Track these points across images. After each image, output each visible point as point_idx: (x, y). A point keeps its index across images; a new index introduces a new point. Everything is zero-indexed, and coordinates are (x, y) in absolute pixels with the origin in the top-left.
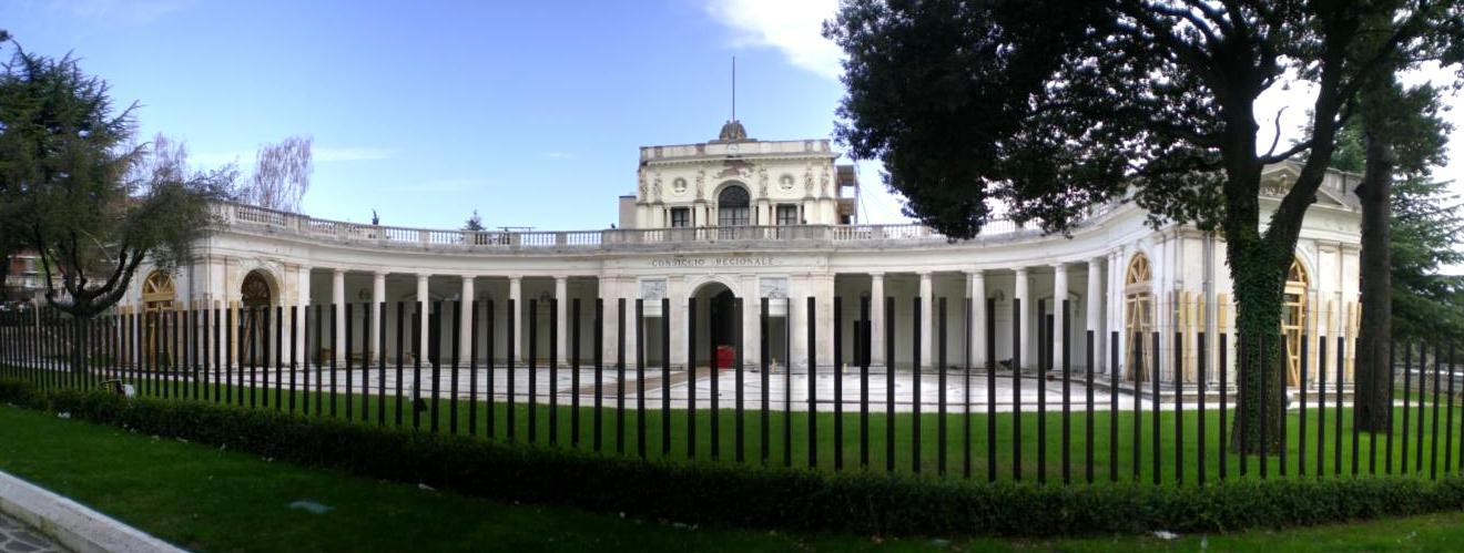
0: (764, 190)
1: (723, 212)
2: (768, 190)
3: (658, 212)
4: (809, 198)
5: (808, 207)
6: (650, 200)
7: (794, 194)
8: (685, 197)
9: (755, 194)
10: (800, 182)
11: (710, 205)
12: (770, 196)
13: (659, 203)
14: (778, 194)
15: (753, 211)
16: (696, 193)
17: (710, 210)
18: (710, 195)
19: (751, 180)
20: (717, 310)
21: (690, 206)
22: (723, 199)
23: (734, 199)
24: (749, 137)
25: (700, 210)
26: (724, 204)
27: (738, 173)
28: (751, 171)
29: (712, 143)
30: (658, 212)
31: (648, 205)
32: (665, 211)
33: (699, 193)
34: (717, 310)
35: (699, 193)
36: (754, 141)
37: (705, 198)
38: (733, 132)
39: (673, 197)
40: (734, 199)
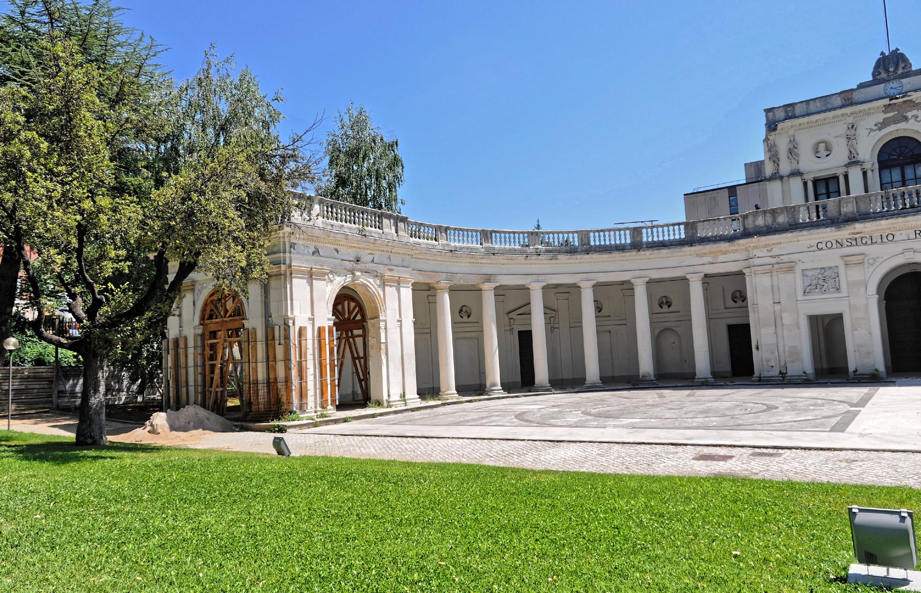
1: (886, 173)
3: (796, 183)
8: (833, 164)
11: (867, 166)
13: (796, 173)
16: (847, 153)
17: (869, 174)
21: (840, 172)
22: (886, 157)
24: (914, 68)
25: (855, 175)
27: (906, 119)
29: (861, 86)
30: (796, 184)
31: (781, 178)
32: (805, 184)
37: (860, 158)
38: (891, 65)
39: (814, 167)
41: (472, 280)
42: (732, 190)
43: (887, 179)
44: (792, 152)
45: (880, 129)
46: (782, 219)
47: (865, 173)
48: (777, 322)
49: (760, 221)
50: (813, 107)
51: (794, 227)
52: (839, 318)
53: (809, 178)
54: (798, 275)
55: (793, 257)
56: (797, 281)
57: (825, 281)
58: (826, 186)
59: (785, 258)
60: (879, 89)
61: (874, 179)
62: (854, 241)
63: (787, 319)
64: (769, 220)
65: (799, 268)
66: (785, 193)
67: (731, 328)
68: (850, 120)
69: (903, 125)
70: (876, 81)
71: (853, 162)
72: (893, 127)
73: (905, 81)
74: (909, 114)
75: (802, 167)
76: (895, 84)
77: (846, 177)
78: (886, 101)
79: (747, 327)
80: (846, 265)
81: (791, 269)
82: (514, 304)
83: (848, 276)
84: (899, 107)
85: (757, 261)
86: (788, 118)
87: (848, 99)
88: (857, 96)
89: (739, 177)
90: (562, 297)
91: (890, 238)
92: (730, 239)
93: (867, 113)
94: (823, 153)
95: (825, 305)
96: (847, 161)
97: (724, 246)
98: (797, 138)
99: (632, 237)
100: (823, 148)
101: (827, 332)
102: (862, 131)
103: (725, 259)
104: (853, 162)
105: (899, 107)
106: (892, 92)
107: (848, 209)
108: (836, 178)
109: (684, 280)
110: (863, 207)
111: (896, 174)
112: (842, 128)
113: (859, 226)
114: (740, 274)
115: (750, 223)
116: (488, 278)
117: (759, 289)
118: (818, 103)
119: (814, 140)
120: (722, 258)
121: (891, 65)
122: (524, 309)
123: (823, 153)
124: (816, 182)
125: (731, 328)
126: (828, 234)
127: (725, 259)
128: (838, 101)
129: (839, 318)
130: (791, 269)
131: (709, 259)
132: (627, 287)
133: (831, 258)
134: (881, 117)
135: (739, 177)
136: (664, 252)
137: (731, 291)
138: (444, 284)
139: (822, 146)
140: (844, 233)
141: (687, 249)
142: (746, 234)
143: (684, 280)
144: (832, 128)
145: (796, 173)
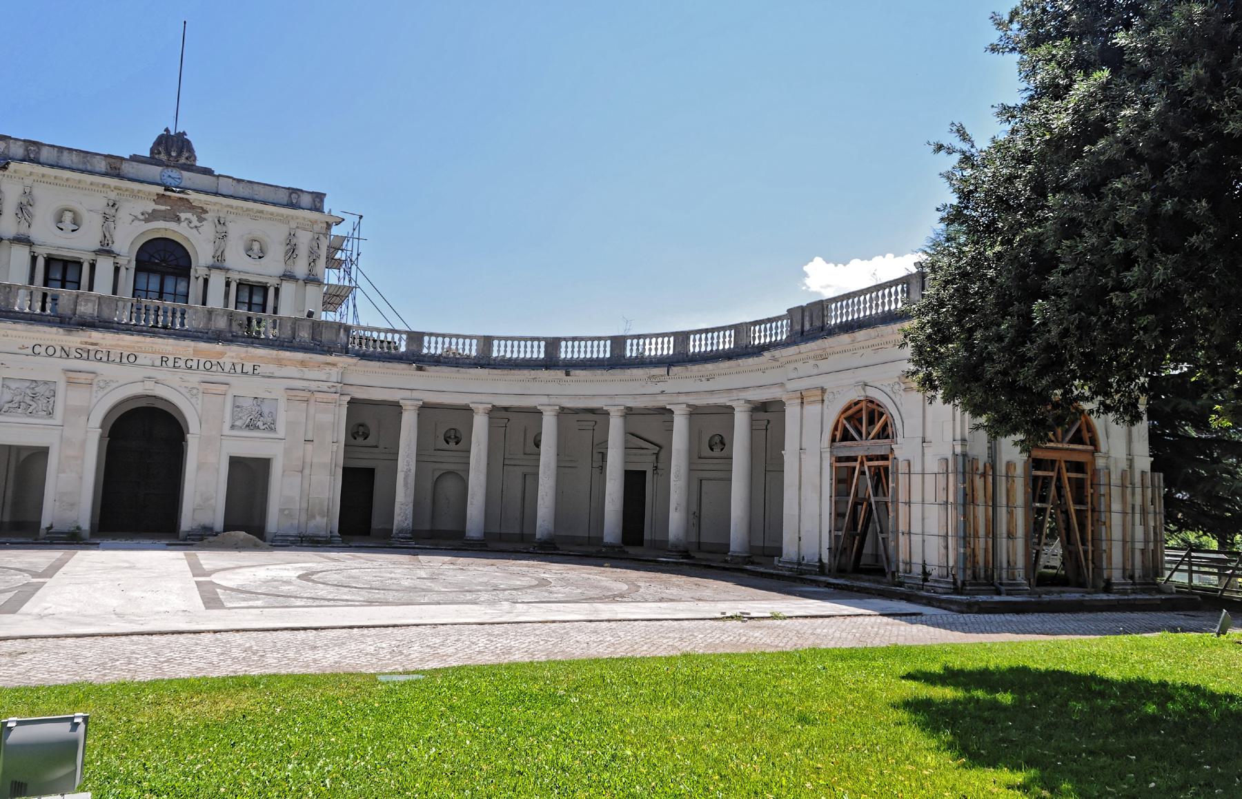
1: (143, 278)
2: (227, 254)
3: (21, 255)
4: (288, 277)
5: (287, 289)
7: (266, 270)
8: (79, 244)
9: (202, 256)
10: (276, 253)
11: (122, 261)
12: (227, 264)
14: (242, 265)
15: (195, 288)
16: (99, 237)
17: (123, 272)
19: (199, 243)
21: (86, 258)
22: (146, 257)
23: (163, 262)
24: (198, 164)
25: (105, 268)
27: (178, 220)
28: (201, 220)
29: (135, 158)
30: (21, 255)
32: (34, 259)
36: (207, 172)
37: (115, 248)
38: (173, 148)
39: (52, 240)
40: (163, 262)
43: (142, 284)
44: (23, 209)
45: (147, 221)
47: (117, 270)
50: (66, 159)
52: (41, 453)
53: (42, 252)
58: (62, 270)
60: (154, 171)
61: (127, 279)
62: (84, 354)
68: (113, 195)
69: (172, 225)
70: (152, 160)
71: (105, 251)
72: (161, 224)
73: (186, 174)
74: (183, 216)
75: (35, 234)
76: (175, 173)
77: (93, 267)
78: (161, 190)
80: (70, 382)
83: (65, 398)
84: (173, 202)
87: (115, 167)
88: (127, 168)
91: (129, 359)
93: (135, 195)
96: (98, 246)
98: (36, 192)
100: (68, 219)
102: (124, 215)
104: (105, 251)
105: (173, 202)
106: (169, 181)
107: (87, 309)
108: (79, 264)
110: (106, 313)
112: (99, 202)
113: (95, 336)
118: (74, 157)
121: (173, 148)
124: (49, 260)
128: (102, 166)
129: (41, 453)
133: (51, 370)
134: (151, 206)
139: (68, 217)
140: (75, 340)
144: (89, 195)
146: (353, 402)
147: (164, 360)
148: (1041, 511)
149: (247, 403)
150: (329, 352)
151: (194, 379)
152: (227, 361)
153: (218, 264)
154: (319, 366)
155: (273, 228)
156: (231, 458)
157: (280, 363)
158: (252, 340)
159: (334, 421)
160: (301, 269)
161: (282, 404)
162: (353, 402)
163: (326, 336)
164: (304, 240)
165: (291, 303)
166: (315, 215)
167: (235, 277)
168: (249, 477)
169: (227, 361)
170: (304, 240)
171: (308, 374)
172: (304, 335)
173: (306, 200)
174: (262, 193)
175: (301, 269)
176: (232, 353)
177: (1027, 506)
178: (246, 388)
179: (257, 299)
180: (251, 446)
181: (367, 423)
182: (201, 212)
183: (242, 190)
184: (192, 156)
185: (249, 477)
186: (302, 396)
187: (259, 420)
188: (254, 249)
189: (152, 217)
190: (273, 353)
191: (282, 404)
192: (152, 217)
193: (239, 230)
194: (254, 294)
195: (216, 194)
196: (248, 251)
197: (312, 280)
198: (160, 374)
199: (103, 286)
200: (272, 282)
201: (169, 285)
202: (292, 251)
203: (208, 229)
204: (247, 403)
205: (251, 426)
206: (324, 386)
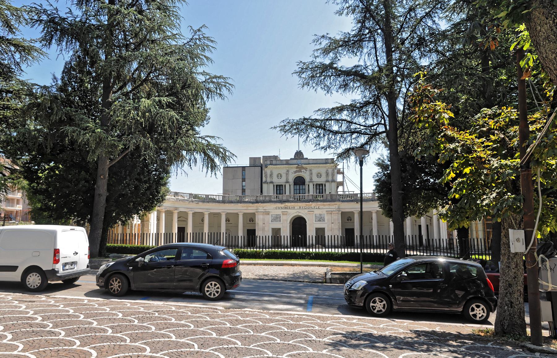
0: (311, 179)
1: (295, 186)
3: (271, 185)
4: (327, 181)
5: (327, 184)
6: (269, 180)
7: (322, 180)
8: (282, 181)
9: (307, 179)
10: (324, 175)
11: (291, 184)
13: (272, 182)
14: (316, 180)
15: (307, 187)
18: (291, 179)
19: (306, 176)
20: (299, 225)
21: (283, 184)
23: (299, 182)
24: (305, 157)
26: (295, 183)
27: (301, 172)
29: (291, 159)
30: (271, 185)
33: (287, 179)
34: (299, 225)
35: (287, 179)
36: (307, 159)
38: (299, 154)
39: (277, 181)
40: (299, 182)
41: (171, 209)
42: (244, 168)
44: (271, 175)
46: (267, 199)
48: (263, 229)
49: (261, 199)
51: (270, 201)
53: (275, 184)
54: (270, 216)
55: (269, 210)
56: (269, 218)
57: (277, 218)
58: (279, 189)
59: (267, 211)
60: (295, 161)
61: (292, 187)
62: (286, 208)
63: (266, 229)
64: (264, 199)
65: (271, 214)
66: (268, 189)
67: (249, 231)
69: (300, 173)
70: (295, 159)
71: (287, 182)
72: (297, 174)
76: (300, 161)
79: (255, 230)
81: (269, 214)
82: (183, 217)
83: (283, 218)
84: (300, 168)
85: (260, 211)
86: (271, 164)
87: (287, 162)
88: (290, 162)
89: (247, 163)
90: (199, 217)
91: (293, 208)
92: (253, 203)
93: (292, 168)
94: (279, 177)
95: (276, 225)
97: (251, 205)
99: (223, 198)
100: (279, 176)
101: (276, 232)
102: (290, 173)
103: (250, 208)
105: (300, 168)
107: (284, 198)
108: (282, 185)
109: (237, 215)
111: (298, 187)
112: (285, 171)
113: (287, 204)
114: (254, 214)
115: (258, 199)
116: (176, 209)
117: (259, 219)
119: (277, 173)
120: (249, 208)
122: (186, 221)
123: (279, 177)
124: (277, 186)
125: (249, 231)
126: (279, 205)
127: (250, 208)
128: (285, 163)
130: (269, 214)
131: (245, 208)
132: (218, 215)
133: (279, 212)
134: (295, 170)
135: (247, 163)
136: (232, 204)
137: (251, 218)
138: (164, 210)
140: (283, 205)
141: (239, 204)
142: (257, 202)
143: (237, 215)
144: (282, 170)
145: (272, 182)
146: (343, 213)
147: (300, 207)
148: (488, 232)
149: (318, 215)
150: (335, 201)
151: (306, 211)
152: (313, 206)
153: (311, 181)
154: (333, 205)
155: (322, 169)
156: (316, 228)
157: (324, 205)
158: (318, 201)
159: (338, 218)
160: (330, 179)
161: (326, 215)
162: (343, 213)
163: (334, 197)
164: (330, 171)
165: (329, 189)
166: (332, 165)
167: (315, 183)
168: (320, 232)
169: (313, 206)
170: (330, 171)
171: (331, 207)
172: (329, 198)
173: (330, 161)
174: (319, 162)
175: (330, 179)
176: (313, 204)
177: (484, 231)
178: (317, 212)
179: (321, 188)
180: (320, 225)
181: (347, 217)
182: (306, 169)
183: (314, 162)
184: (303, 156)
185: (320, 232)
186: (330, 213)
187: (321, 219)
188: (319, 175)
189: (295, 172)
190: (322, 203)
191: (326, 215)
192: (295, 172)
193: (315, 172)
194: (320, 187)
195: (309, 164)
196: (318, 175)
197: (333, 181)
198: (300, 211)
199: (288, 193)
200: (324, 183)
201: (301, 188)
202: (327, 174)
203: (308, 172)
204: (318, 215)
205: (320, 221)
206: (335, 210)
